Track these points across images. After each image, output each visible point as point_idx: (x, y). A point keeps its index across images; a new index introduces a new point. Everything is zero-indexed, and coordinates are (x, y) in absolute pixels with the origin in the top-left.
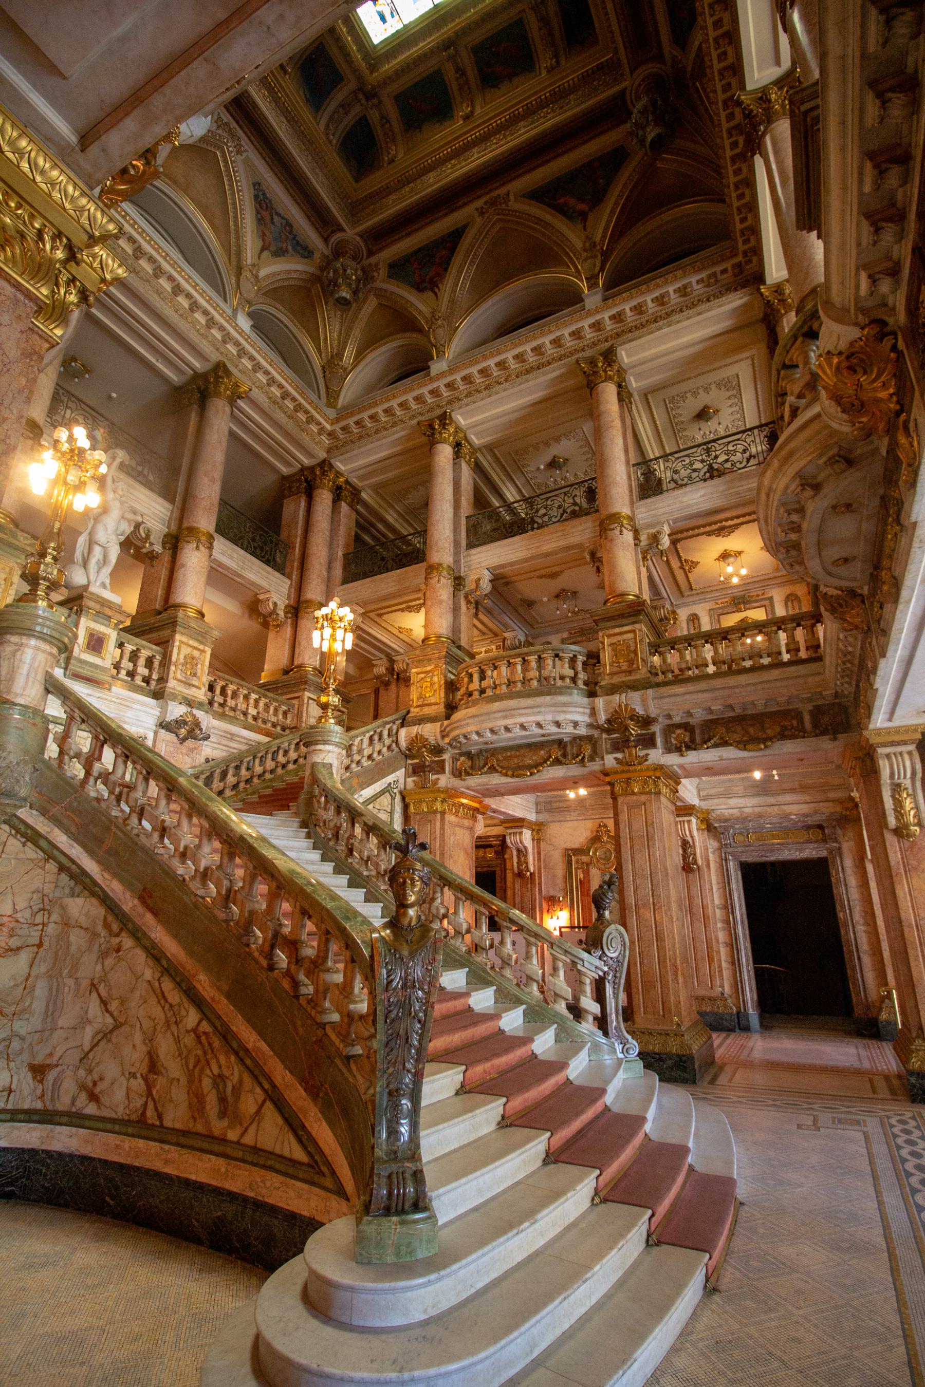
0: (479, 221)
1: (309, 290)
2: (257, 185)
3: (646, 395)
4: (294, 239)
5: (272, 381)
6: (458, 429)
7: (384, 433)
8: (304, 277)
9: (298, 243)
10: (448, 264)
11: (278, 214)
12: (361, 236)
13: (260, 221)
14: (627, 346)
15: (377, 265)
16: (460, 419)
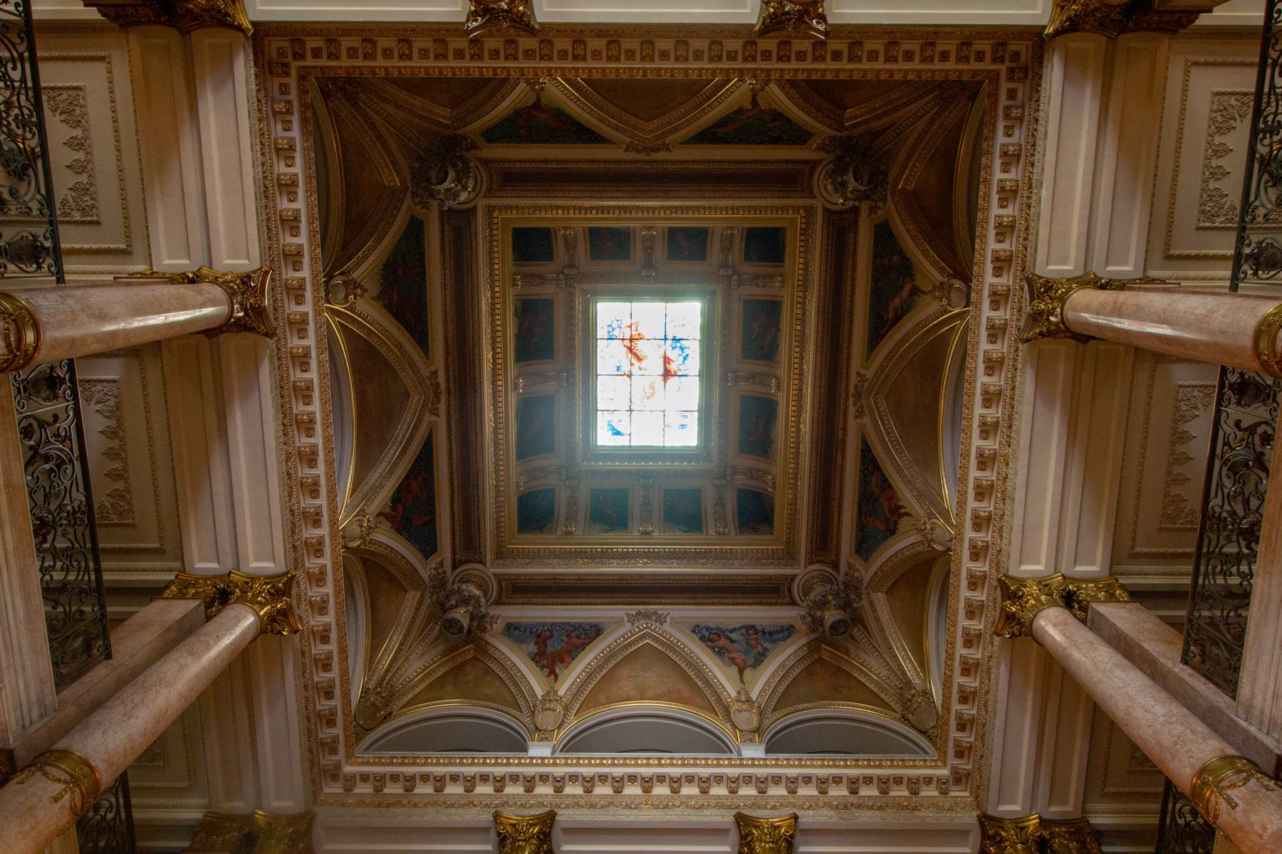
0: (866, 420)
1: (821, 660)
2: (696, 629)
3: (1169, 257)
4: (764, 633)
5: (823, 784)
6: (1044, 584)
7: (990, 697)
8: (801, 654)
9: (771, 634)
10: (886, 480)
11: (734, 630)
12: (812, 563)
13: (720, 652)
14: (1041, 256)
15: (850, 566)
16: (1033, 568)
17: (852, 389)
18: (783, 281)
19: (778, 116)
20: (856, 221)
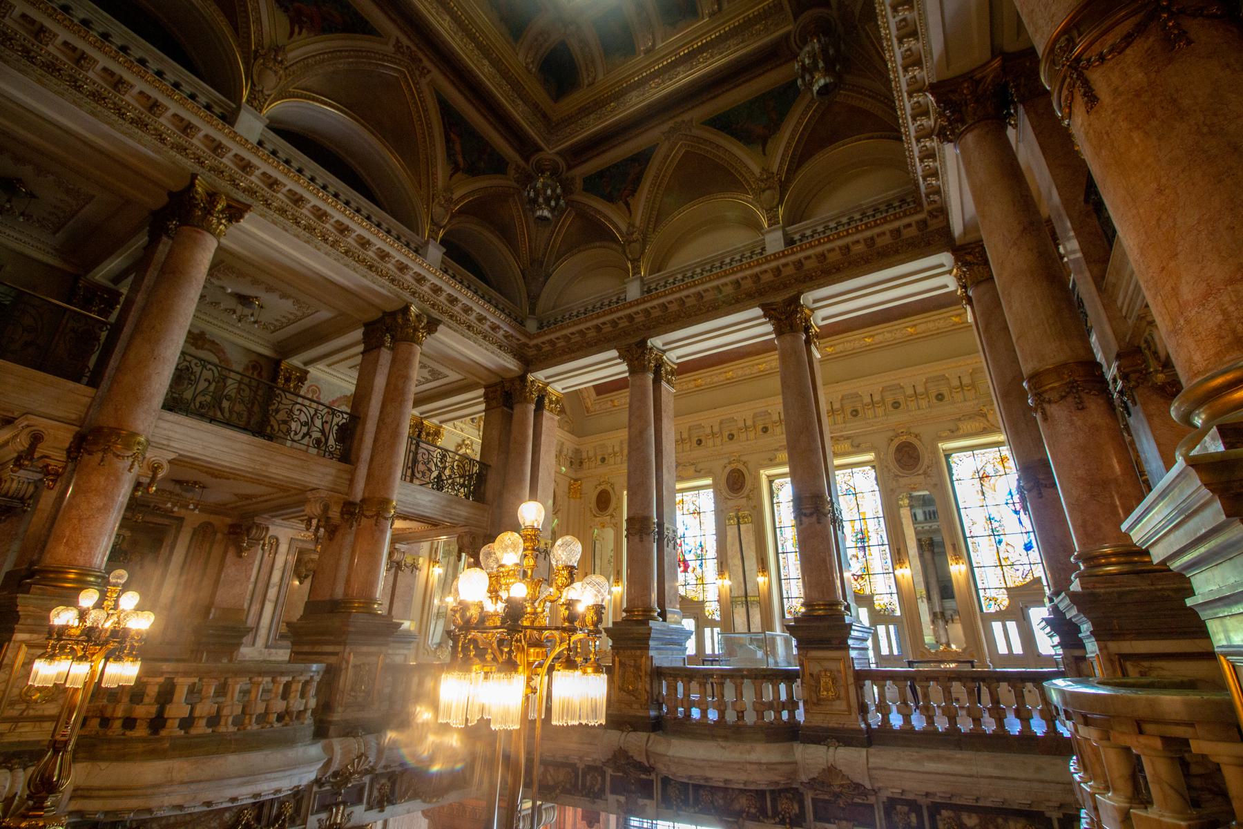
0: (390, 49)
17: (421, 55)
18: (529, 71)
19: (610, 199)
20: (521, 155)
